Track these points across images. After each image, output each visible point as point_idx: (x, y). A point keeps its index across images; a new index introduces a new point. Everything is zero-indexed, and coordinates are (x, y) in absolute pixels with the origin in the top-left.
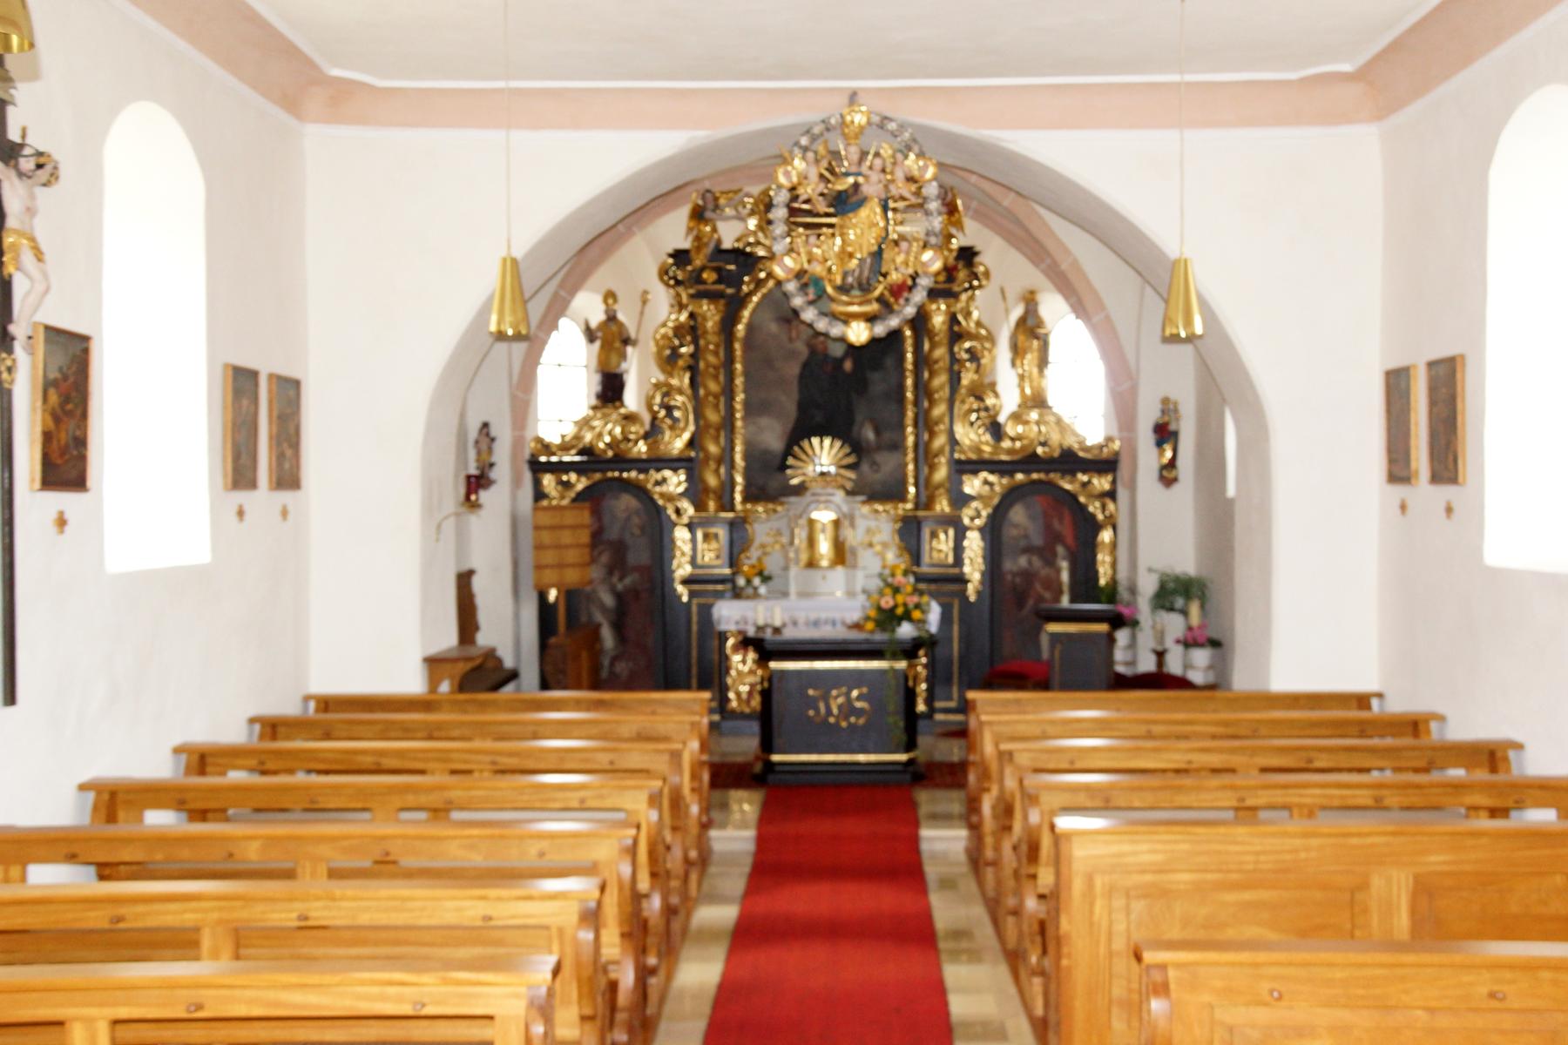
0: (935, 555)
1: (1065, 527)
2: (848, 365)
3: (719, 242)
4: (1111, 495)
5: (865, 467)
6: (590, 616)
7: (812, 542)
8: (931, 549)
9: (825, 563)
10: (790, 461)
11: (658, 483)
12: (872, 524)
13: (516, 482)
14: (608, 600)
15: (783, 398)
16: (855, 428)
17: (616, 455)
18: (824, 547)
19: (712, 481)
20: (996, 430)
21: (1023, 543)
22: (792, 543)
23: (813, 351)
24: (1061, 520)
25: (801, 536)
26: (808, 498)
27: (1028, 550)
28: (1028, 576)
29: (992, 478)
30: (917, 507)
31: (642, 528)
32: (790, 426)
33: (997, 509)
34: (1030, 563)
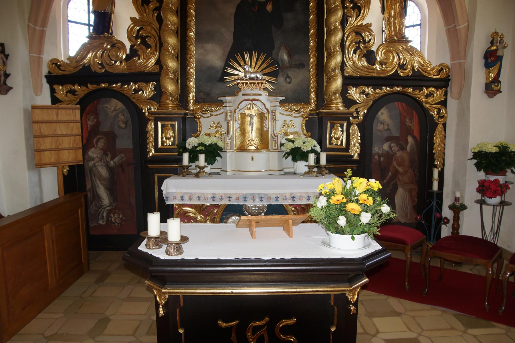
0: (334, 141)
1: (414, 124)
4: (444, 103)
5: (281, 79)
6: (92, 182)
7: (243, 132)
9: (253, 148)
10: (230, 71)
12: (288, 119)
13: (37, 91)
14: (104, 172)
16: (274, 52)
17: (106, 70)
18: (253, 135)
19: (171, 87)
20: (370, 56)
21: (386, 134)
22: (228, 133)
24: (411, 120)
25: (236, 126)
26: (240, 97)
27: (389, 139)
28: (389, 156)
29: (369, 90)
30: (318, 107)
31: (126, 123)
32: (228, 50)
34: (390, 147)
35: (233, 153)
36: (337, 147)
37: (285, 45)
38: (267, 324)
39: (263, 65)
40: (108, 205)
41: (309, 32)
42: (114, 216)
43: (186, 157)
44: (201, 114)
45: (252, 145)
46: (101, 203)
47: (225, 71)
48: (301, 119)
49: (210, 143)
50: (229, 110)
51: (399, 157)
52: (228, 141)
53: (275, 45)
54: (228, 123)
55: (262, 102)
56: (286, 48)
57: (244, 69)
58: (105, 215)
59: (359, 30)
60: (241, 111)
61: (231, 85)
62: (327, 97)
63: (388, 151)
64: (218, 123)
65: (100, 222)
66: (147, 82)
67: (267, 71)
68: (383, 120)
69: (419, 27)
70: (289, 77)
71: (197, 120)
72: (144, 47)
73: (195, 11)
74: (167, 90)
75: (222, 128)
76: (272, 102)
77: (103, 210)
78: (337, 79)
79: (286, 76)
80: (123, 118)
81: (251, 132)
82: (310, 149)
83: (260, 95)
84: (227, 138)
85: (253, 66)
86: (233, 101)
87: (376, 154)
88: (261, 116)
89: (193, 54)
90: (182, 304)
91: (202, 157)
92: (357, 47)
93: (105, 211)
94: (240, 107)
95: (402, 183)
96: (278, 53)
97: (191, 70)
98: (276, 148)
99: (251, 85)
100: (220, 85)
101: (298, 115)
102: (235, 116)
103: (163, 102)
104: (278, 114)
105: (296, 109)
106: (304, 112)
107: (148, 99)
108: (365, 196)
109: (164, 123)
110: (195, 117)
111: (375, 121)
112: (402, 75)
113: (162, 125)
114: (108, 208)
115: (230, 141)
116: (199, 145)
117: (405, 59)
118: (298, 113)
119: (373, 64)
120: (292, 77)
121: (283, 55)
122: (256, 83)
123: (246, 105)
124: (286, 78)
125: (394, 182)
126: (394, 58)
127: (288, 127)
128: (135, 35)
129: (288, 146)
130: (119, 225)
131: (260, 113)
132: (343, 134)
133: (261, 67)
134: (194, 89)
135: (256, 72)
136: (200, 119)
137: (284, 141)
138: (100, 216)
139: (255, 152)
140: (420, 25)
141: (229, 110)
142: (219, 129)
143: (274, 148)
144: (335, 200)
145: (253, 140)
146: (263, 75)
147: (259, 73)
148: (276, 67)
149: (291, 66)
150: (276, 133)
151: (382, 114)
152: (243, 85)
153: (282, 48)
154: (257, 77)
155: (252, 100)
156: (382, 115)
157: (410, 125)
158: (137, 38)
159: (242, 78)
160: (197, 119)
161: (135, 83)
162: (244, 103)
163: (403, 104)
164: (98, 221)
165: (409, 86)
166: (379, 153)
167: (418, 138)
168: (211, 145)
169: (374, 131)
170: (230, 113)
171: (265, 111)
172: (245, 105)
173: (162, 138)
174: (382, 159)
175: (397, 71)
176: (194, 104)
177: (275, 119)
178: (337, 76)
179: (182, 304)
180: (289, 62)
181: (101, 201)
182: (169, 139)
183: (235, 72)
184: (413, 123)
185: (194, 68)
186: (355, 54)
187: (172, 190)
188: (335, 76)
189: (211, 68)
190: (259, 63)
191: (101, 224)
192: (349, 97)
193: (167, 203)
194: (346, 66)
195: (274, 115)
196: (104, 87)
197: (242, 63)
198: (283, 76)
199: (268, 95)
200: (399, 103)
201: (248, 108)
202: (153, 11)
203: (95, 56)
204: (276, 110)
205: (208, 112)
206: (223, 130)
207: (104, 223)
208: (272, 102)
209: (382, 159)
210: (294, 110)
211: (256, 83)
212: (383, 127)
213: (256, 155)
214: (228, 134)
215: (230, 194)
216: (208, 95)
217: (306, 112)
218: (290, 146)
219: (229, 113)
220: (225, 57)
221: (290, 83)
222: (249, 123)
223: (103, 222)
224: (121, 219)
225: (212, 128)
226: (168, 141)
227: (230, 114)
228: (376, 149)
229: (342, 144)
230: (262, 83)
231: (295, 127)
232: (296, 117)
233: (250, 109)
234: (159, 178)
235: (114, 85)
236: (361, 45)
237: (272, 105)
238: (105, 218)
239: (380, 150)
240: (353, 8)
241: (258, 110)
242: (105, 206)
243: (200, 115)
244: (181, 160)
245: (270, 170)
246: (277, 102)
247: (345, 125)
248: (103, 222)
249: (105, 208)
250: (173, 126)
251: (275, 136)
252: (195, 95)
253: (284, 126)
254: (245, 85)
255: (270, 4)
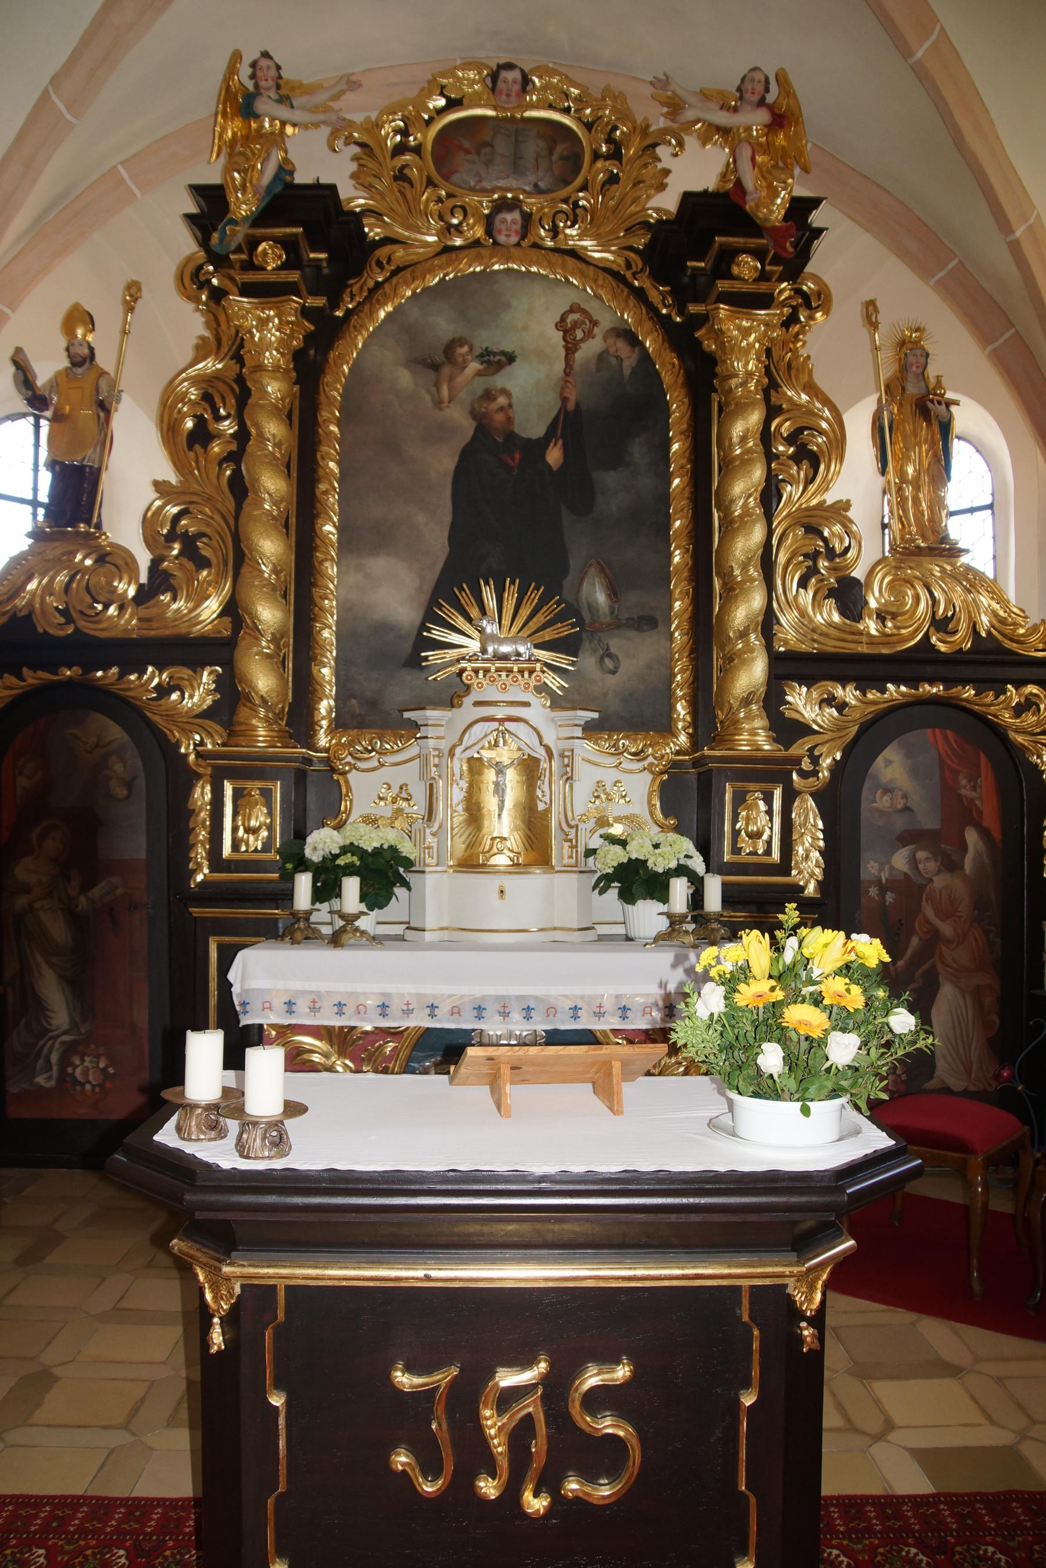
0: (746, 845)
2: (554, 456)
3: (285, 170)
7: (474, 814)
8: (736, 833)
9: (502, 860)
10: (438, 634)
11: (163, 691)
12: (609, 776)
15: (421, 518)
16: (568, 583)
17: (77, 629)
21: (900, 824)
23: (482, 428)
24: (973, 779)
26: (467, 711)
27: (910, 837)
29: (849, 694)
30: (696, 742)
32: (433, 576)
33: (848, 750)
34: (913, 862)
35: (446, 875)
36: (754, 859)
37: (599, 563)
38: (545, 1380)
39: (535, 619)
40: (66, 1027)
41: (668, 526)
42: (83, 1061)
43: (304, 883)
44: (353, 762)
45: (500, 852)
46: (45, 1024)
47: (425, 634)
48: (648, 777)
49: (376, 844)
50: (435, 749)
51: (941, 893)
52: (429, 839)
53: (571, 563)
54: (431, 785)
55: (531, 726)
56: (602, 570)
57: (481, 631)
58: (54, 1058)
59: (813, 521)
60: (469, 754)
61: (441, 676)
62: (722, 710)
63: (906, 874)
64: (401, 788)
65: (41, 1080)
66: (197, 665)
67: (548, 635)
68: (891, 781)
69: (989, 512)
70: (610, 656)
71: (341, 777)
72: (190, 565)
73: (338, 463)
74: (254, 688)
75: (412, 803)
76: (560, 726)
77: (50, 1042)
78: (753, 659)
79: (601, 652)
80: (122, 769)
81: (499, 815)
82: (673, 865)
83: (527, 704)
84: (428, 831)
85: (506, 621)
86: (448, 722)
87: (871, 883)
88: (530, 768)
89: (331, 586)
90: (281, 1316)
91: (351, 886)
92: (808, 568)
93: (57, 1046)
94: (467, 740)
95: (950, 970)
96: (581, 584)
97: (326, 634)
98: (573, 861)
99: (500, 676)
100: (409, 677)
101: (640, 765)
102: (452, 768)
103: (240, 723)
104: (578, 762)
105: (633, 750)
106: (655, 758)
107: (197, 716)
108: (839, 984)
109: (241, 784)
110: (333, 770)
111: (867, 784)
112: (942, 647)
113: (235, 790)
114: (66, 1038)
115: (436, 840)
116: (345, 850)
117: (949, 602)
118: (638, 760)
119: (858, 618)
120: (620, 655)
121: (595, 592)
122: (515, 669)
123: (486, 735)
124: (602, 659)
125: (927, 965)
126: (917, 599)
127: (609, 800)
128: (165, 531)
129: (610, 857)
130: (97, 1090)
131: (526, 757)
132: (771, 820)
133: (530, 623)
134: (332, 687)
135: (514, 640)
136: (349, 776)
137: (595, 842)
138: (41, 1061)
139: (510, 873)
140: (990, 507)
141: (435, 749)
142: (405, 804)
143: (566, 861)
144: (747, 994)
145: (505, 839)
146: (537, 646)
147: (524, 641)
148: (573, 626)
149: (617, 625)
150: (574, 819)
151: (888, 763)
152: (477, 677)
153: (592, 571)
154: (519, 654)
155: (501, 721)
156: (886, 767)
157: (973, 794)
158: (171, 538)
159: (475, 655)
160: (340, 774)
161: (160, 668)
162: (478, 730)
163: (948, 732)
164: (34, 1078)
165: (964, 682)
166: (880, 881)
167: (997, 835)
168: (378, 852)
169: (864, 815)
170: (438, 756)
171: (541, 753)
172: (483, 735)
173: (235, 830)
174: (889, 897)
175: (927, 636)
176: (331, 731)
177: (569, 775)
178: (752, 651)
179: (281, 1316)
180: (612, 612)
181: (47, 1017)
182: (254, 831)
183: (455, 638)
184: (979, 790)
185: (334, 628)
186: (805, 588)
187: (258, 983)
188: (745, 653)
189: (383, 628)
190: (525, 612)
191: (42, 1087)
192: (787, 714)
193: (245, 1021)
194: (779, 623)
195: (568, 766)
196: (70, 677)
197: (474, 612)
198: (594, 651)
199: (548, 704)
200: (937, 730)
201: (489, 743)
202: (220, 464)
203: (48, 590)
204: (572, 751)
205: (374, 753)
206: (415, 808)
207: (52, 1084)
208: (560, 726)
209: (889, 897)
210: (626, 749)
211: (515, 669)
212: (892, 804)
213: (515, 884)
214: (429, 819)
215: (435, 997)
216: (373, 704)
217: (663, 756)
218: (616, 856)
219: (434, 756)
220: (425, 598)
221: (613, 672)
222: (492, 787)
223: (49, 1079)
224: (104, 1070)
225: (382, 803)
226: (252, 838)
227: (437, 760)
228: (871, 868)
229: (768, 852)
230: (531, 672)
231: (628, 799)
232: (631, 772)
233: (496, 745)
234: (221, 948)
235: (99, 674)
236: (823, 564)
237: (561, 735)
238: (55, 1068)
239: (883, 869)
240: (797, 459)
241: (519, 749)
242: (55, 1033)
243: (348, 764)
244: (288, 896)
245: (555, 929)
246: (576, 725)
247: (778, 793)
248: (49, 1079)
249: (55, 1038)
250: (267, 795)
251: (570, 827)
252: (336, 706)
253: (598, 797)
254: (481, 675)
255: (555, 445)
